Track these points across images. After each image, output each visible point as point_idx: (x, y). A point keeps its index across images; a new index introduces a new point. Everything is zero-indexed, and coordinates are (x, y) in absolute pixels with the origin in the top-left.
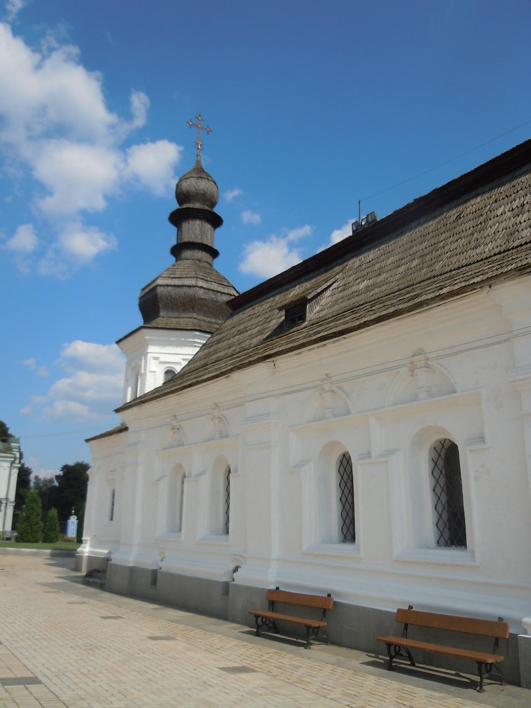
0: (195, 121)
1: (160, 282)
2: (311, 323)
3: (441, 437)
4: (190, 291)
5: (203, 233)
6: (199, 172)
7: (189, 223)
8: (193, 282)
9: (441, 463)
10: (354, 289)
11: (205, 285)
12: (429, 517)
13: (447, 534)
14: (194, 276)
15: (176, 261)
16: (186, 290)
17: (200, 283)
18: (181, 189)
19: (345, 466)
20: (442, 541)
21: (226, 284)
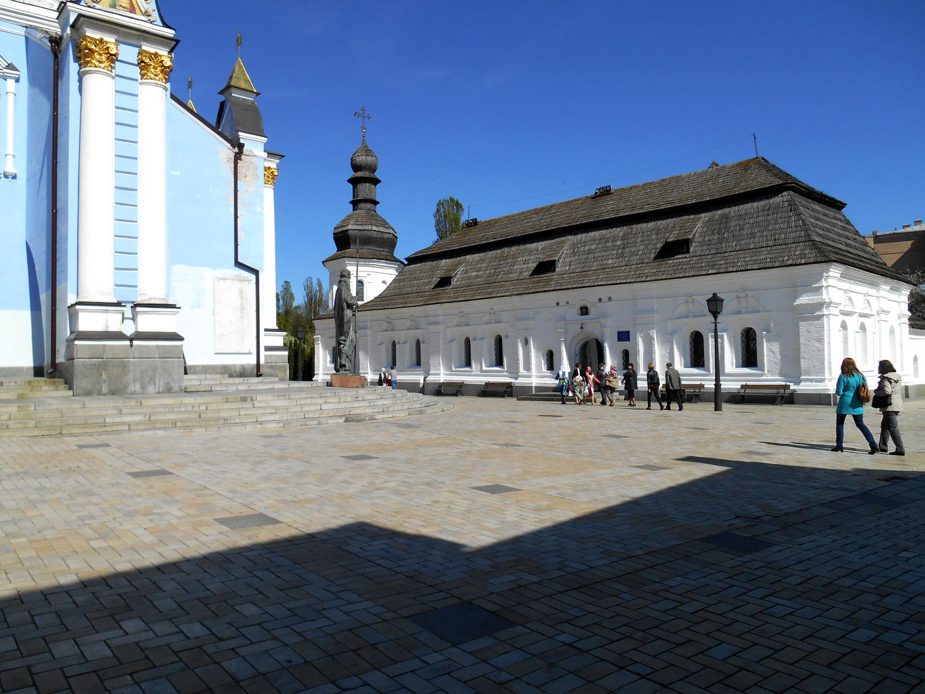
1: (350, 227)
4: (368, 233)
5: (371, 192)
8: (369, 227)
12: (494, 357)
17: (374, 228)
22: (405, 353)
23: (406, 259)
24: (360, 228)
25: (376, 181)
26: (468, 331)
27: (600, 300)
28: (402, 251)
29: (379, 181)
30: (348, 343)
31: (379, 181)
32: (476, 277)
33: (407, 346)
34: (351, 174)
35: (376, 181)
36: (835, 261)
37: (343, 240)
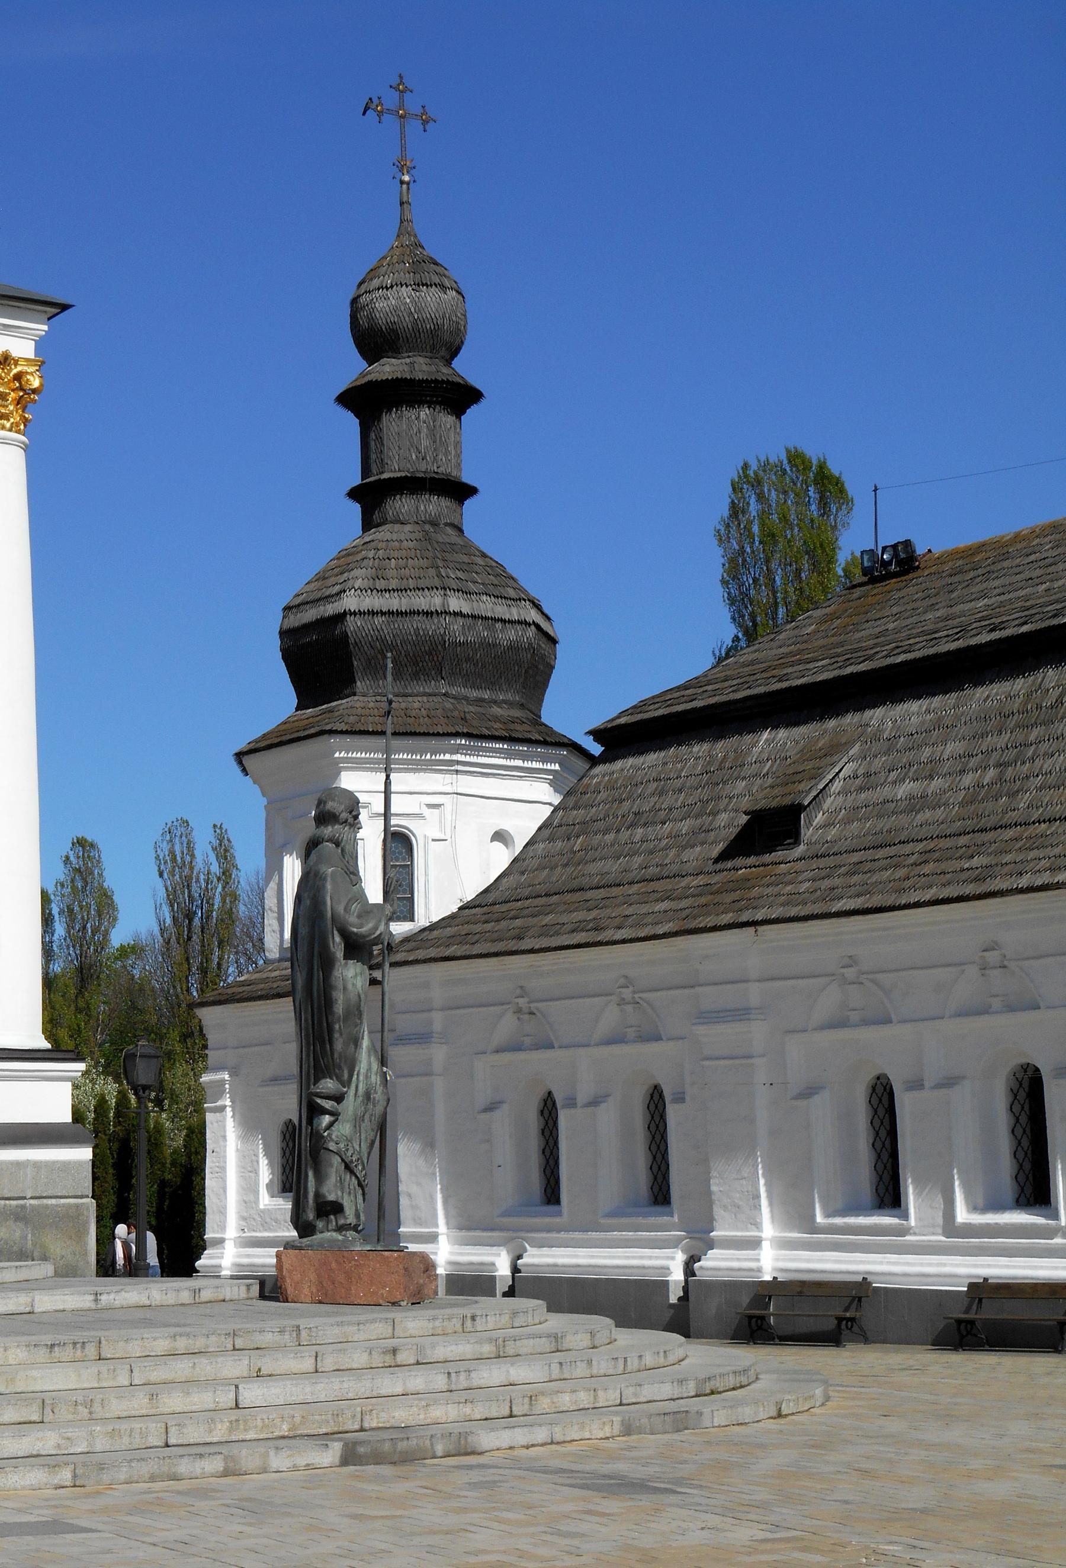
0: (391, 99)
1: (350, 602)
2: (813, 850)
3: (1024, 1060)
4: (431, 626)
7: (400, 417)
8: (435, 601)
9: (1022, 1095)
10: (886, 792)
13: (1029, 1190)
14: (437, 582)
15: (368, 524)
16: (418, 622)
17: (456, 603)
18: (371, 318)
20: (1022, 1199)
21: (512, 593)
22: (600, 1148)
23: (598, 734)
24: (394, 603)
25: (460, 398)
26: (888, 1050)
28: (576, 705)
30: (350, 1105)
32: (916, 804)
33: (607, 1117)
34: (351, 368)
35: (460, 398)
37: (321, 660)
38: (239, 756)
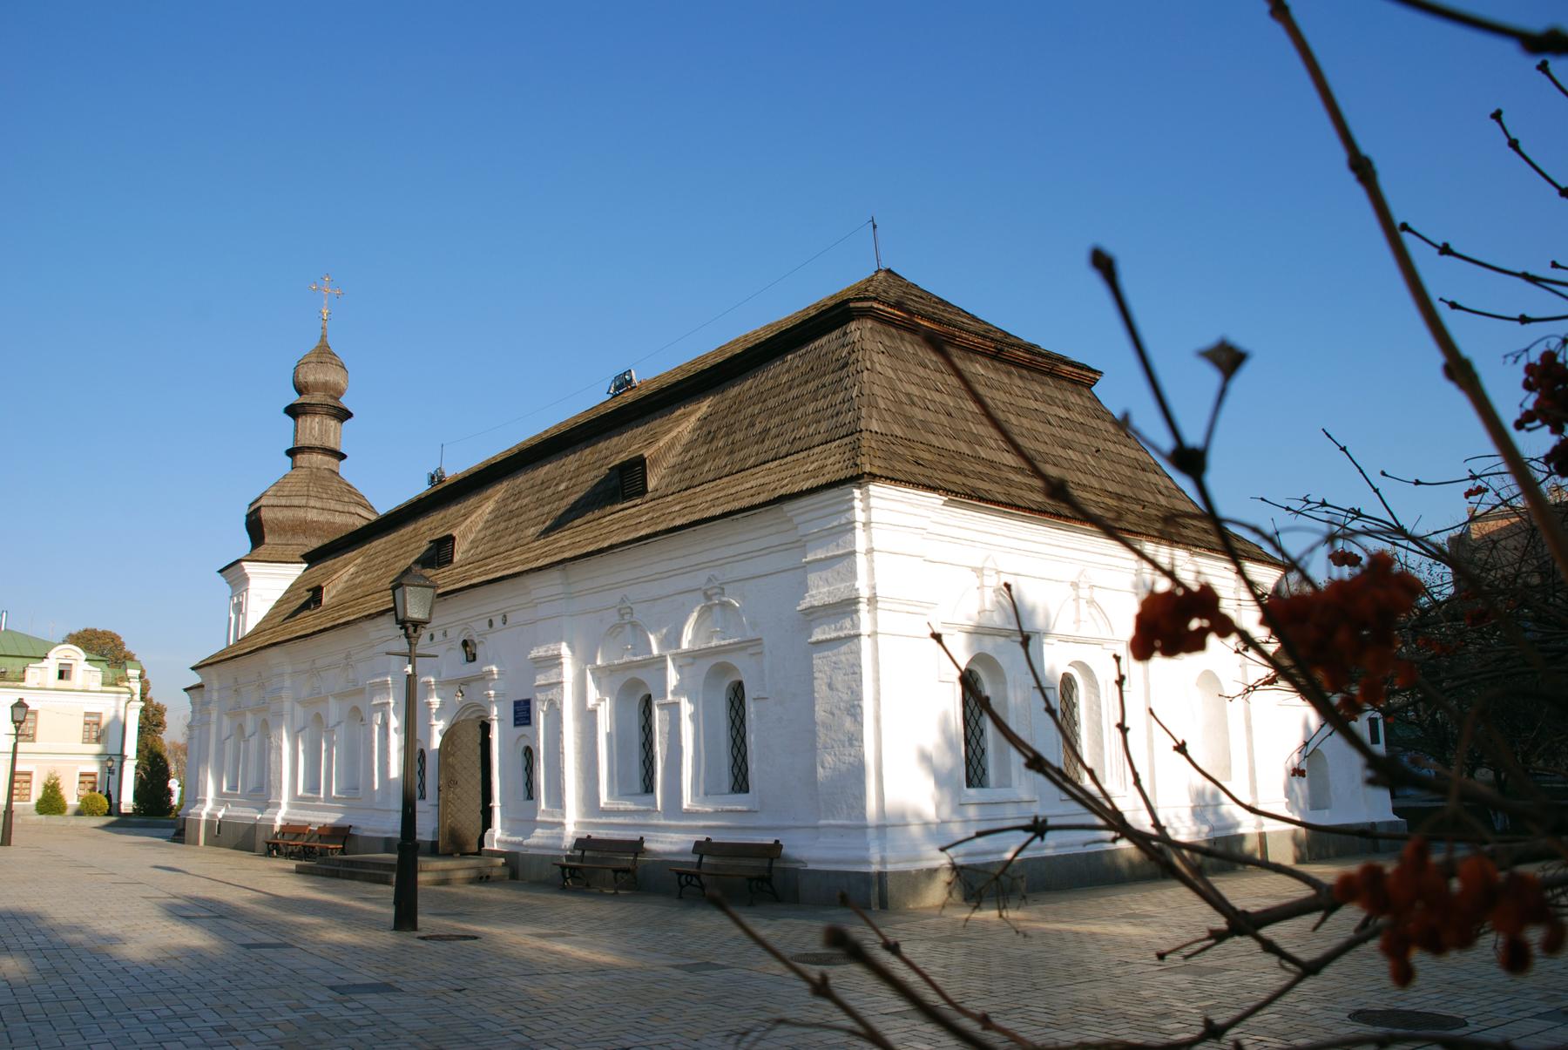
1: (263, 502)
4: (301, 513)
5: (324, 432)
6: (324, 354)
11: (318, 505)
17: (312, 503)
19: (737, 695)
27: (491, 623)
29: (348, 415)
31: (348, 415)
34: (294, 398)
35: (343, 415)
36: (874, 477)
38: (221, 571)
